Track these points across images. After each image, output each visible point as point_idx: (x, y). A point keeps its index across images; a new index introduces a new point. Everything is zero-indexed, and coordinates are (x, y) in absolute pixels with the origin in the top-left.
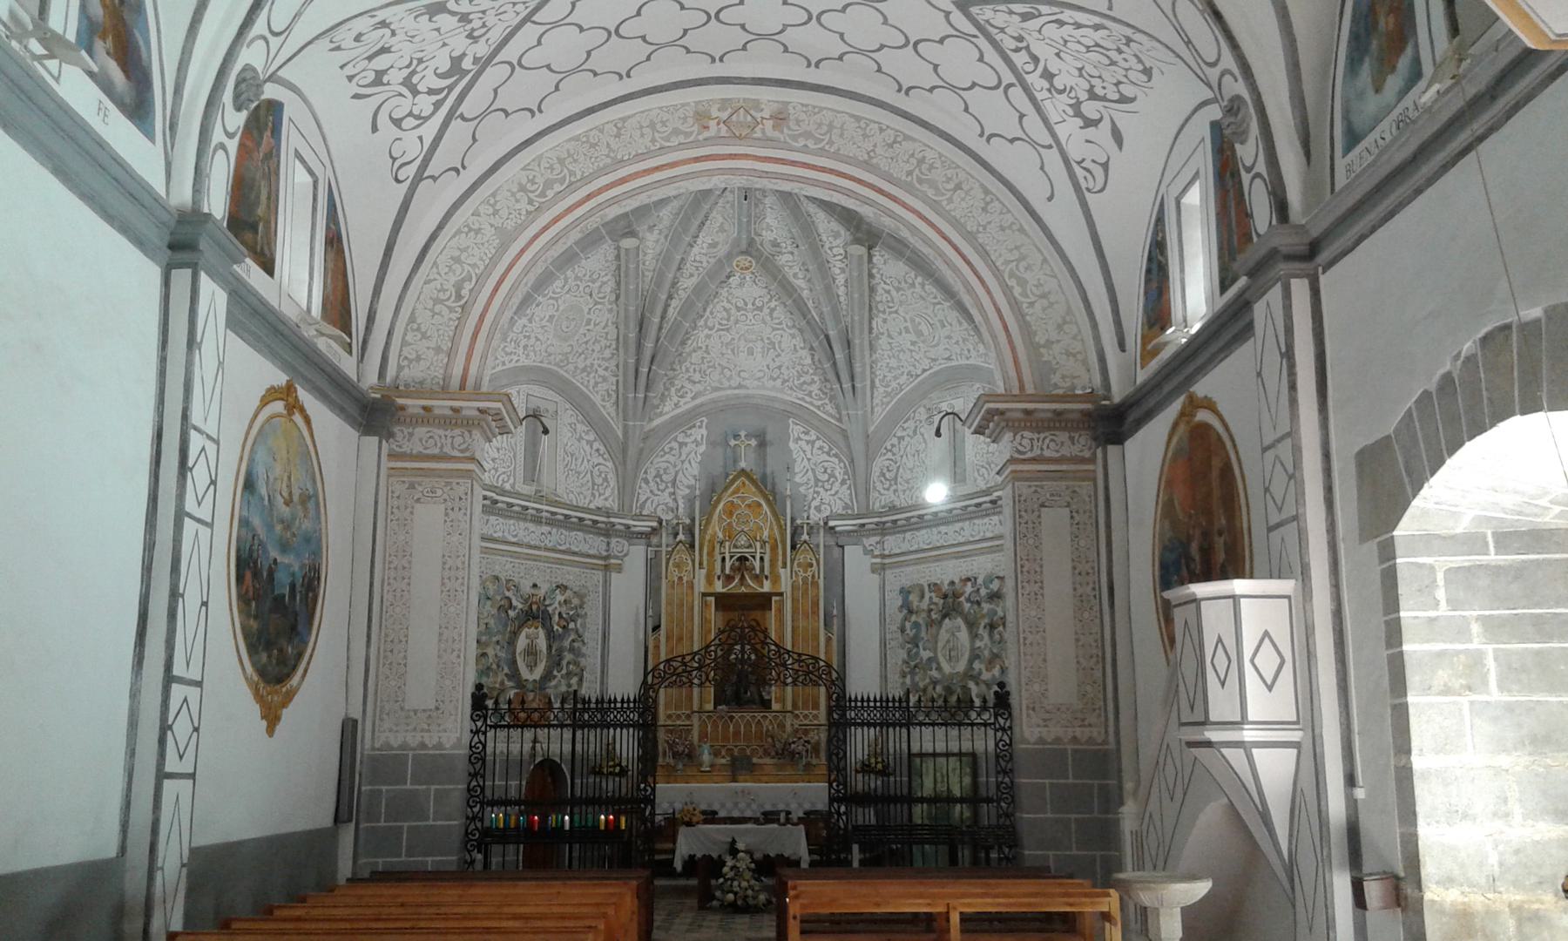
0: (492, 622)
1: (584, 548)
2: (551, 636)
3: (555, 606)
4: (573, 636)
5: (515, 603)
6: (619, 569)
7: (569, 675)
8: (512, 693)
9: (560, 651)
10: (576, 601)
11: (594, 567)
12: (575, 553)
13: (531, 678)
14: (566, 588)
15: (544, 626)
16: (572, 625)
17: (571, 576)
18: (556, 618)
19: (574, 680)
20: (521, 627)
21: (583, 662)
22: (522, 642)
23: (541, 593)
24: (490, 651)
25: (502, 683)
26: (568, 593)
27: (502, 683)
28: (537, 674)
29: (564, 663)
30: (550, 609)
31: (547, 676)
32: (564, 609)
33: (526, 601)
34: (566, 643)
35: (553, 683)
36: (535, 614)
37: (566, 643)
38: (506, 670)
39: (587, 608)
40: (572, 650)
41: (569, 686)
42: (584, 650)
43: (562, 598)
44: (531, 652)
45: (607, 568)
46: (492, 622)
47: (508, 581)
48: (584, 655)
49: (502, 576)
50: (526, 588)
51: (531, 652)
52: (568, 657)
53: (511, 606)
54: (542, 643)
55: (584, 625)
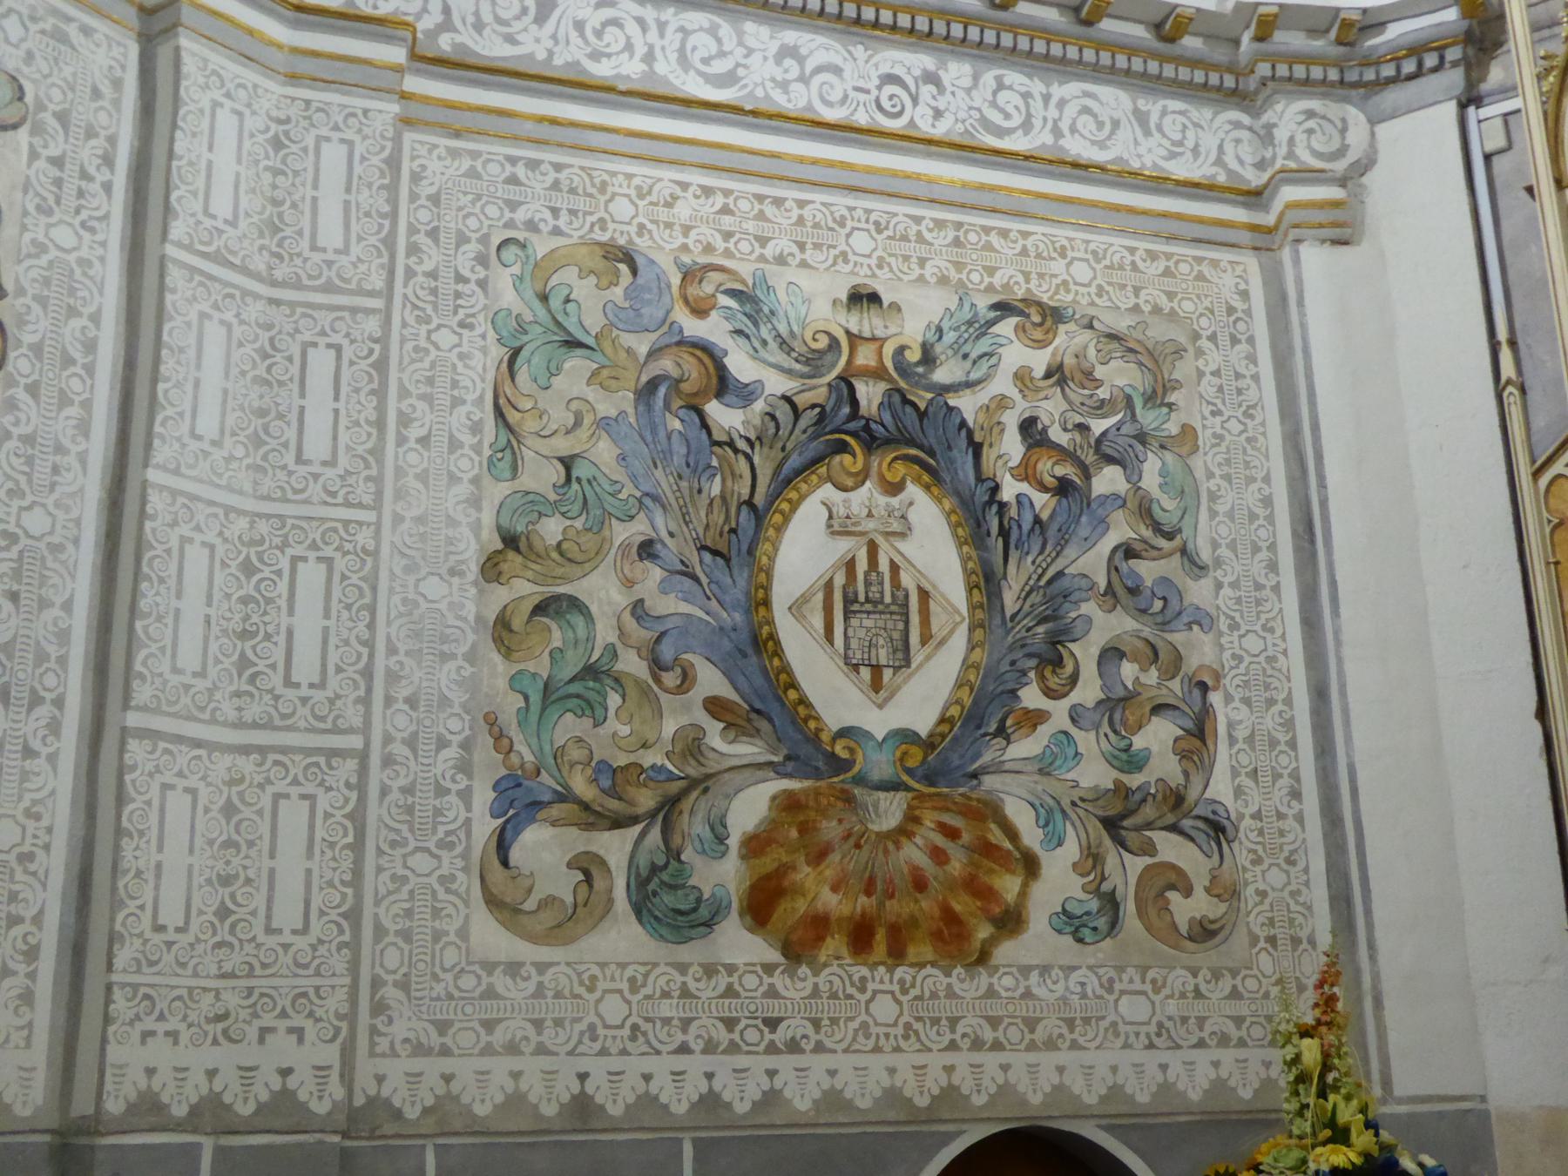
0: (604, 451)
1: (1148, 154)
2: (982, 521)
3: (1000, 385)
4: (1121, 530)
5: (741, 365)
6: (1341, 229)
7: (1118, 709)
8: (749, 808)
9: (1054, 598)
10: (1118, 375)
11: (1210, 237)
12: (1079, 169)
13: (878, 722)
14: (1053, 316)
15: (934, 477)
16: (1108, 480)
17: (1081, 266)
18: (1012, 446)
19: (1157, 737)
20: (788, 482)
21: (1200, 650)
22: (804, 552)
23: (912, 330)
24: (603, 592)
25: (691, 746)
26: (1068, 341)
27: (691, 746)
28: (924, 698)
29: (1085, 653)
30: (968, 405)
31: (985, 712)
32: (1051, 409)
33: (814, 361)
34: (1090, 560)
35: (1026, 747)
36: (881, 421)
37: (1090, 560)
38: (711, 681)
39: (1189, 408)
40: (1122, 591)
41: (1131, 761)
42: (1198, 592)
43: (1039, 361)
44: (871, 602)
45: (1264, 240)
46: (604, 451)
47: (691, 275)
48: (1202, 620)
49: (663, 252)
50: (811, 300)
51: (871, 602)
52: (1105, 624)
53: (723, 384)
54: (932, 549)
55: (1187, 492)
